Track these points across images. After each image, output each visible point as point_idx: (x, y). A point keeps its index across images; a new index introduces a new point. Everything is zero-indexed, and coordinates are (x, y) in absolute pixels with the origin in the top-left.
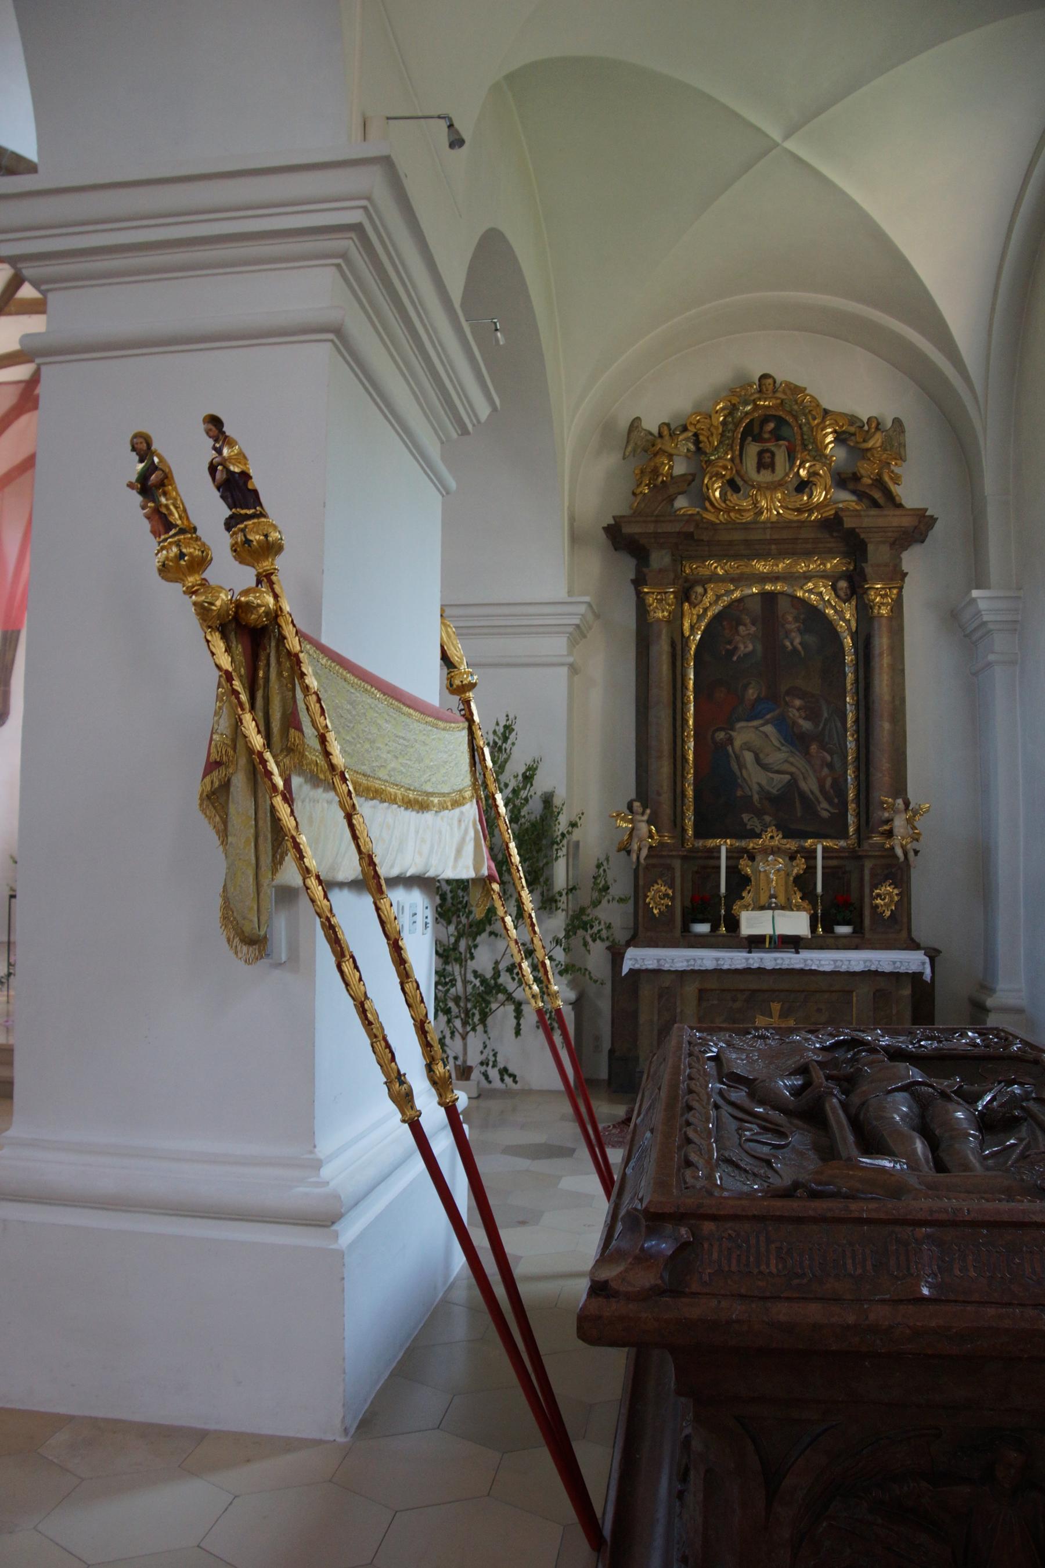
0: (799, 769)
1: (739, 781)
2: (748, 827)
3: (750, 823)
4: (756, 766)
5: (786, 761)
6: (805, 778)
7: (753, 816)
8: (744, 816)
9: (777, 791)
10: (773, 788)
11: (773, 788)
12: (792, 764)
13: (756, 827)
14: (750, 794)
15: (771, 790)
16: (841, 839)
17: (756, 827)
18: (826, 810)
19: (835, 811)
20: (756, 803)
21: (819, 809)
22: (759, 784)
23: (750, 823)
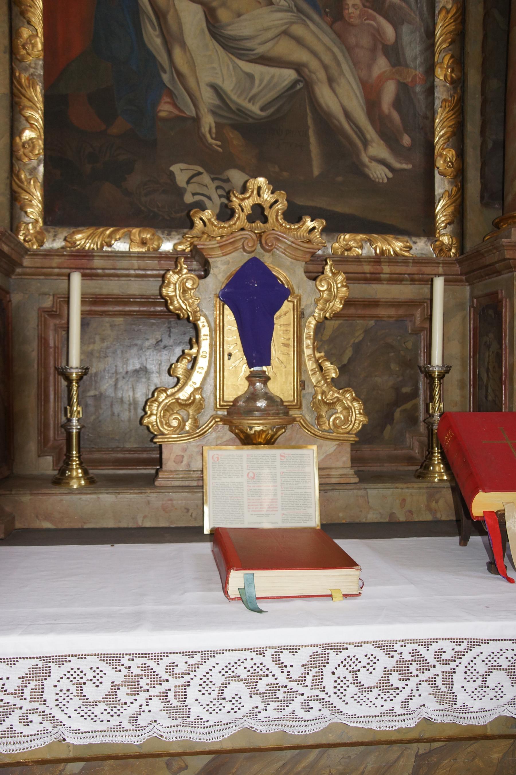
0: (315, 54)
1: (165, 77)
2: (189, 199)
3: (191, 188)
4: (213, 44)
5: (285, 33)
6: (331, 81)
7: (201, 169)
8: (175, 168)
9: (262, 109)
10: (252, 99)
11: (252, 99)
12: (299, 41)
13: (209, 198)
14: (191, 112)
15: (249, 106)
16: (418, 236)
17: (209, 198)
18: (383, 162)
19: (405, 166)
20: (210, 141)
21: (366, 160)
22: (216, 89)
23: (191, 188)
